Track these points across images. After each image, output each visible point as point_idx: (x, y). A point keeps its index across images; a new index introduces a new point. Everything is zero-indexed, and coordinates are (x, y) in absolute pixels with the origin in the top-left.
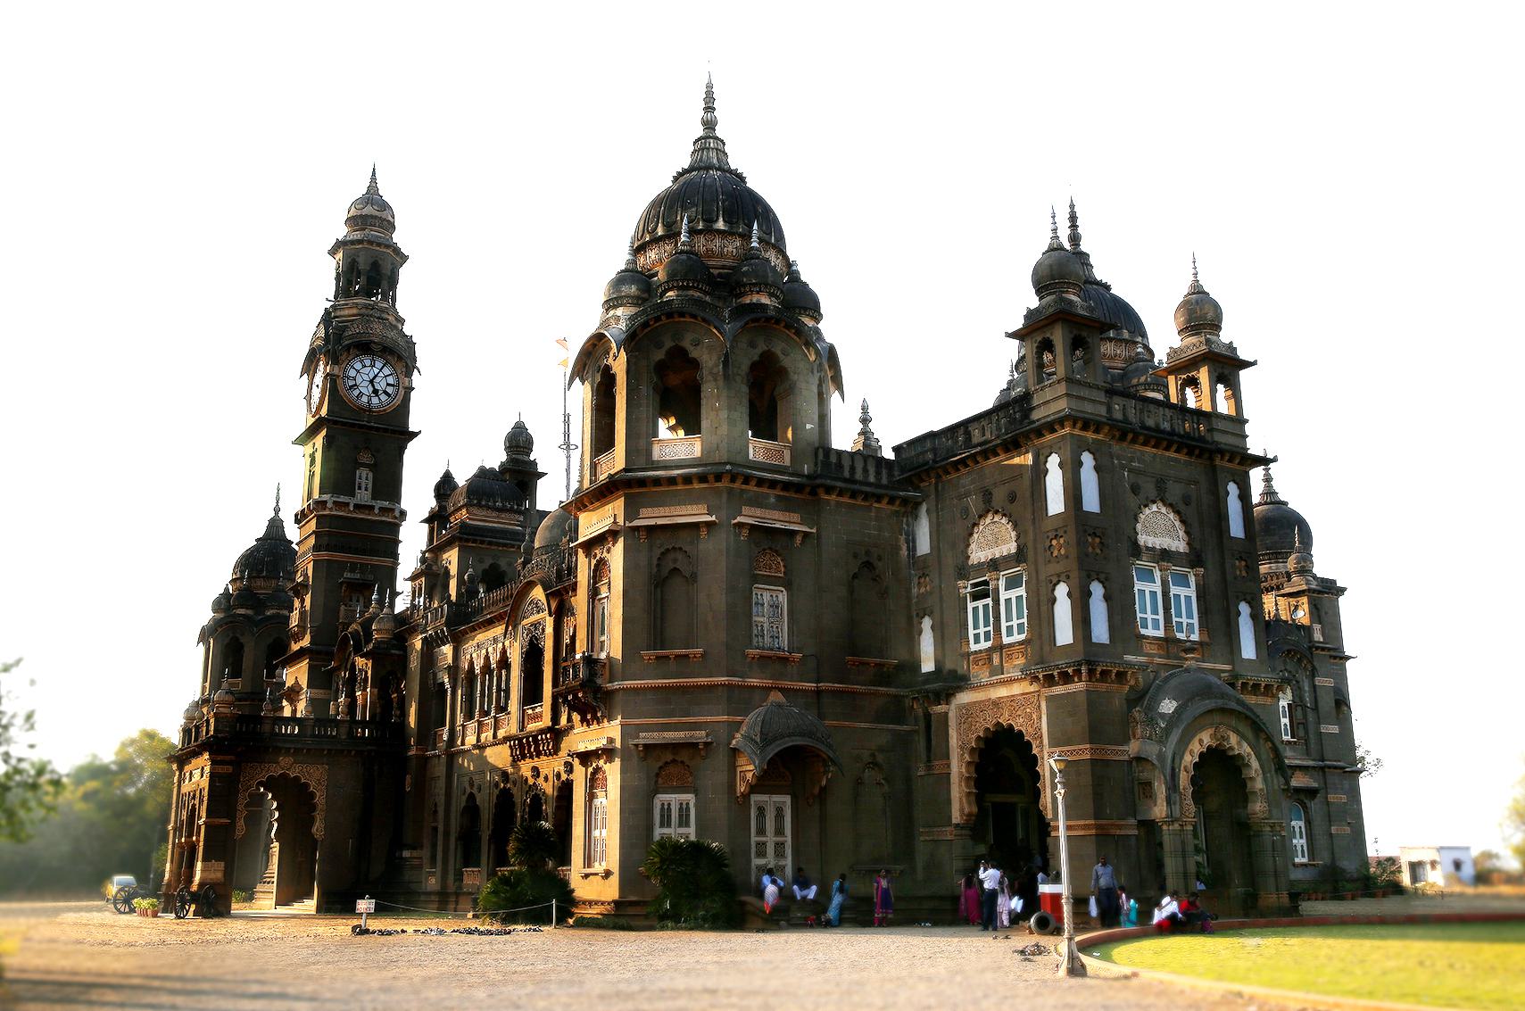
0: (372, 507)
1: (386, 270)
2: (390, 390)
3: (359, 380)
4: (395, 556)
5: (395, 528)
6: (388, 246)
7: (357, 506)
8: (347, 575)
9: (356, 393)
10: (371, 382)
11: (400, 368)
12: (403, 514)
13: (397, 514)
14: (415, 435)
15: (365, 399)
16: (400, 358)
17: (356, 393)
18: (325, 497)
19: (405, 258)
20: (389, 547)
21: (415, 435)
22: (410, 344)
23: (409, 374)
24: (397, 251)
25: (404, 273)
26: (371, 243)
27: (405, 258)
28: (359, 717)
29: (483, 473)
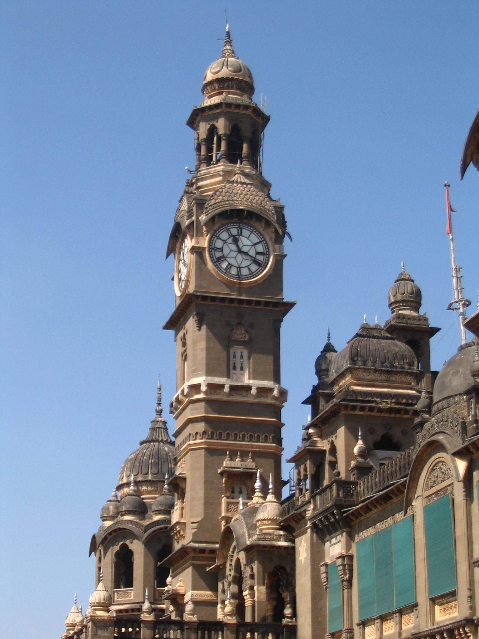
0: (249, 388)
1: (246, 129)
2: (260, 258)
3: (226, 251)
4: (278, 440)
5: (276, 411)
6: (246, 107)
7: (232, 388)
8: (227, 463)
9: (224, 265)
10: (240, 251)
11: (269, 236)
12: (283, 393)
13: (276, 393)
14: (291, 305)
15: (234, 271)
16: (268, 224)
17: (224, 265)
18: (201, 380)
19: (267, 119)
20: (275, 432)
21: (291, 305)
22: (279, 210)
23: (279, 239)
24: (257, 111)
25: (270, 136)
26: (229, 105)
27: (267, 119)
28: (248, 619)
29: (367, 332)
